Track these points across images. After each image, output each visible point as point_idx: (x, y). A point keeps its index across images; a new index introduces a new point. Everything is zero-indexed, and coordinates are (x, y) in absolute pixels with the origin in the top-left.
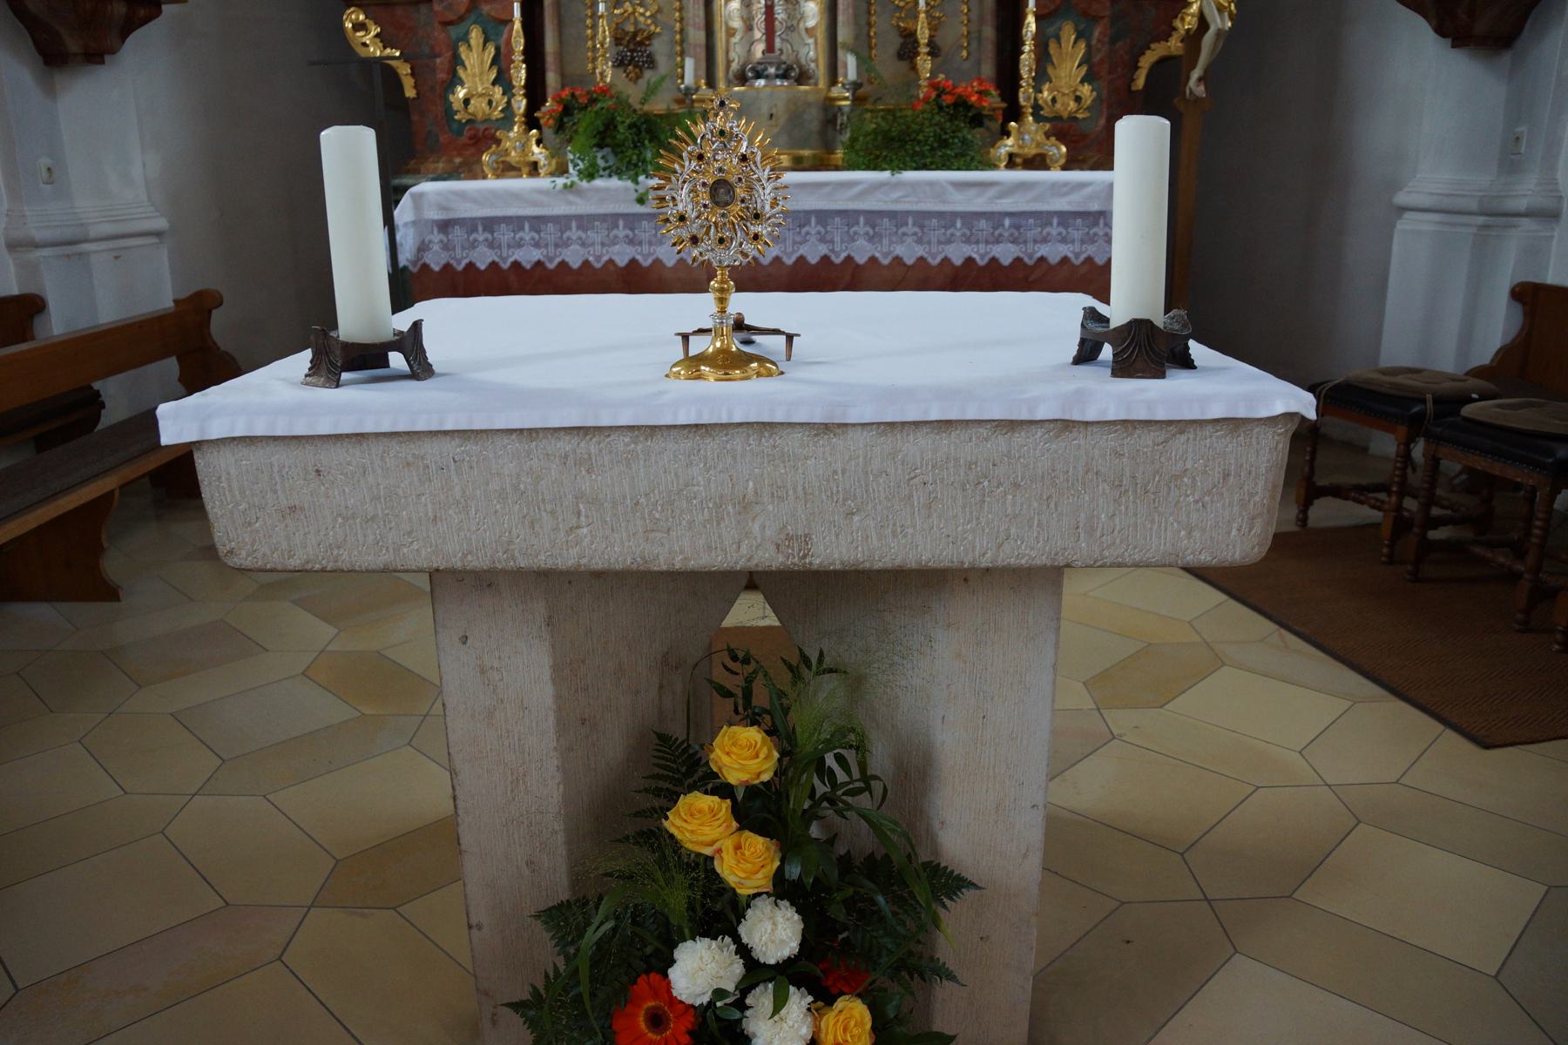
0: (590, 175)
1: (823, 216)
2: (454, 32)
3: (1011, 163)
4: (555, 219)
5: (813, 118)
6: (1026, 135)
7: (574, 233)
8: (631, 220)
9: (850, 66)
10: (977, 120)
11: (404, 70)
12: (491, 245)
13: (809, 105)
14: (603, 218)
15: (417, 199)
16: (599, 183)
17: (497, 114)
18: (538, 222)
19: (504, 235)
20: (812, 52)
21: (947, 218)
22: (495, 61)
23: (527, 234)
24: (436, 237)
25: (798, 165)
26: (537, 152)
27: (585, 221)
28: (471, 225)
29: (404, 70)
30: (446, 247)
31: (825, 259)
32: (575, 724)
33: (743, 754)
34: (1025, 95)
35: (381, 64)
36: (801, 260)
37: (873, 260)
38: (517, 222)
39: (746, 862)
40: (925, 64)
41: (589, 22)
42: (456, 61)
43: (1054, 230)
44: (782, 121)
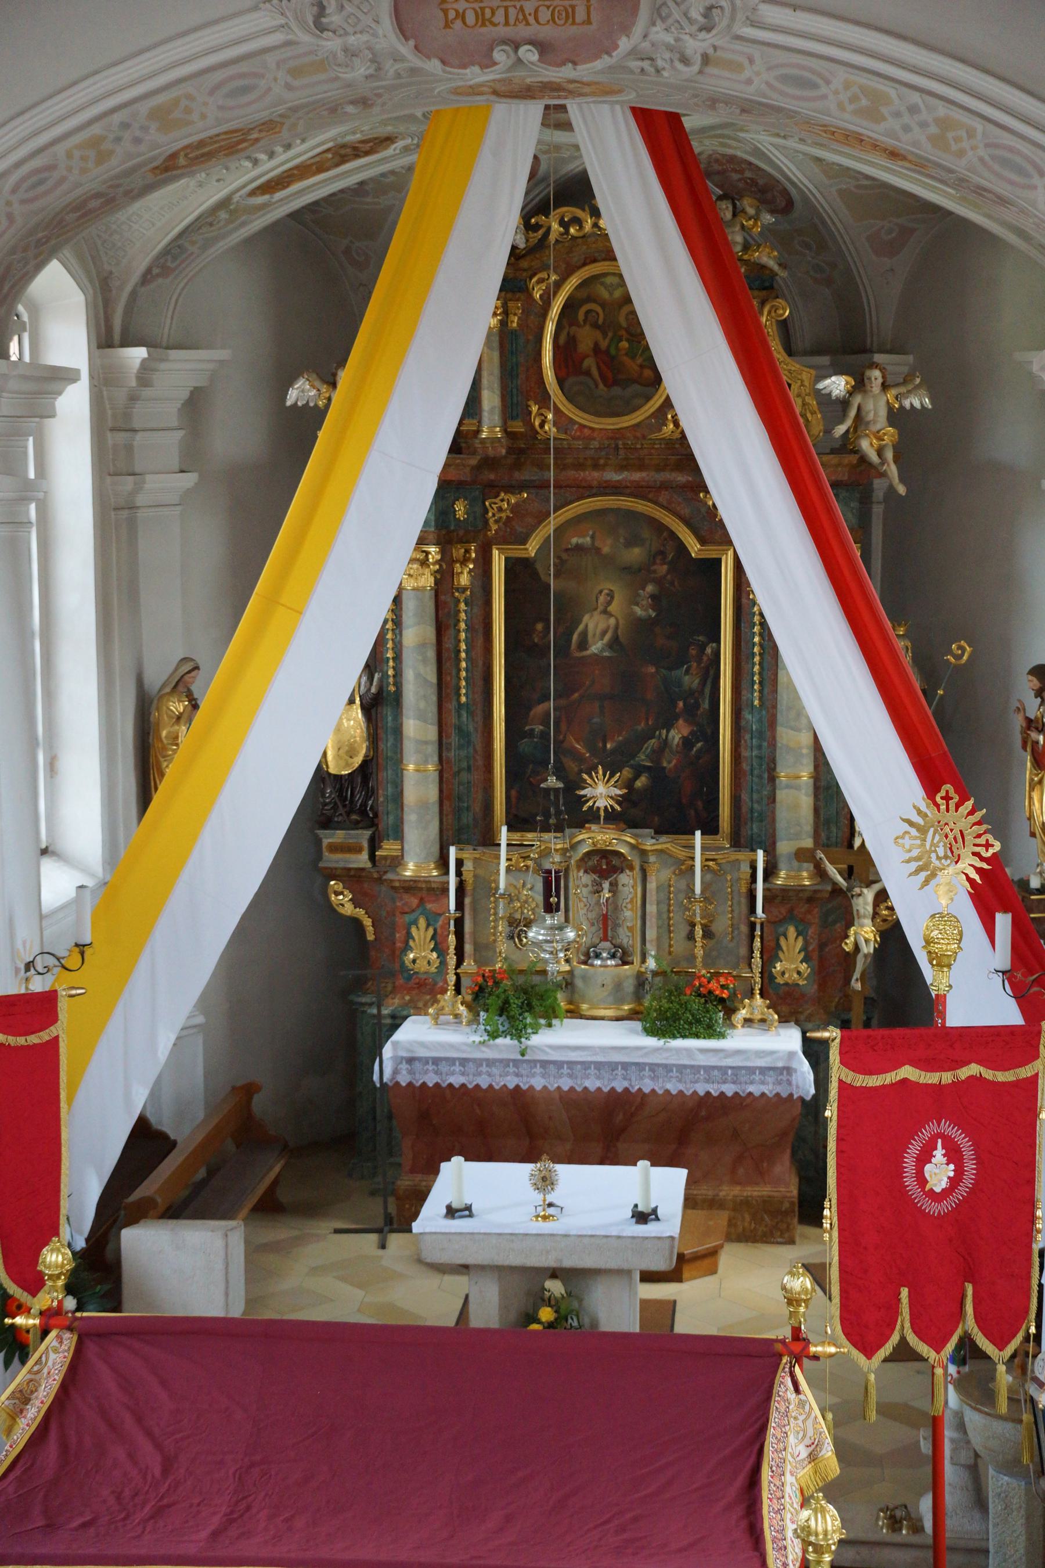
0: (494, 1035)
1: (625, 1066)
2: (407, 918)
4: (474, 1060)
5: (629, 986)
7: (484, 1069)
8: (516, 1063)
11: (367, 922)
12: (436, 1073)
13: (627, 977)
14: (501, 1061)
15: (395, 1044)
16: (500, 1041)
17: (433, 970)
18: (464, 1062)
19: (444, 1067)
21: (696, 1069)
22: (433, 938)
23: (457, 1068)
24: (404, 1066)
27: (490, 1062)
28: (426, 1061)
29: (367, 922)
30: (411, 1072)
31: (626, 1090)
32: (504, 1307)
35: (356, 923)
36: (613, 1089)
37: (653, 1091)
38: (451, 1061)
41: (492, 911)
42: (409, 936)
43: (757, 1077)
44: (610, 988)
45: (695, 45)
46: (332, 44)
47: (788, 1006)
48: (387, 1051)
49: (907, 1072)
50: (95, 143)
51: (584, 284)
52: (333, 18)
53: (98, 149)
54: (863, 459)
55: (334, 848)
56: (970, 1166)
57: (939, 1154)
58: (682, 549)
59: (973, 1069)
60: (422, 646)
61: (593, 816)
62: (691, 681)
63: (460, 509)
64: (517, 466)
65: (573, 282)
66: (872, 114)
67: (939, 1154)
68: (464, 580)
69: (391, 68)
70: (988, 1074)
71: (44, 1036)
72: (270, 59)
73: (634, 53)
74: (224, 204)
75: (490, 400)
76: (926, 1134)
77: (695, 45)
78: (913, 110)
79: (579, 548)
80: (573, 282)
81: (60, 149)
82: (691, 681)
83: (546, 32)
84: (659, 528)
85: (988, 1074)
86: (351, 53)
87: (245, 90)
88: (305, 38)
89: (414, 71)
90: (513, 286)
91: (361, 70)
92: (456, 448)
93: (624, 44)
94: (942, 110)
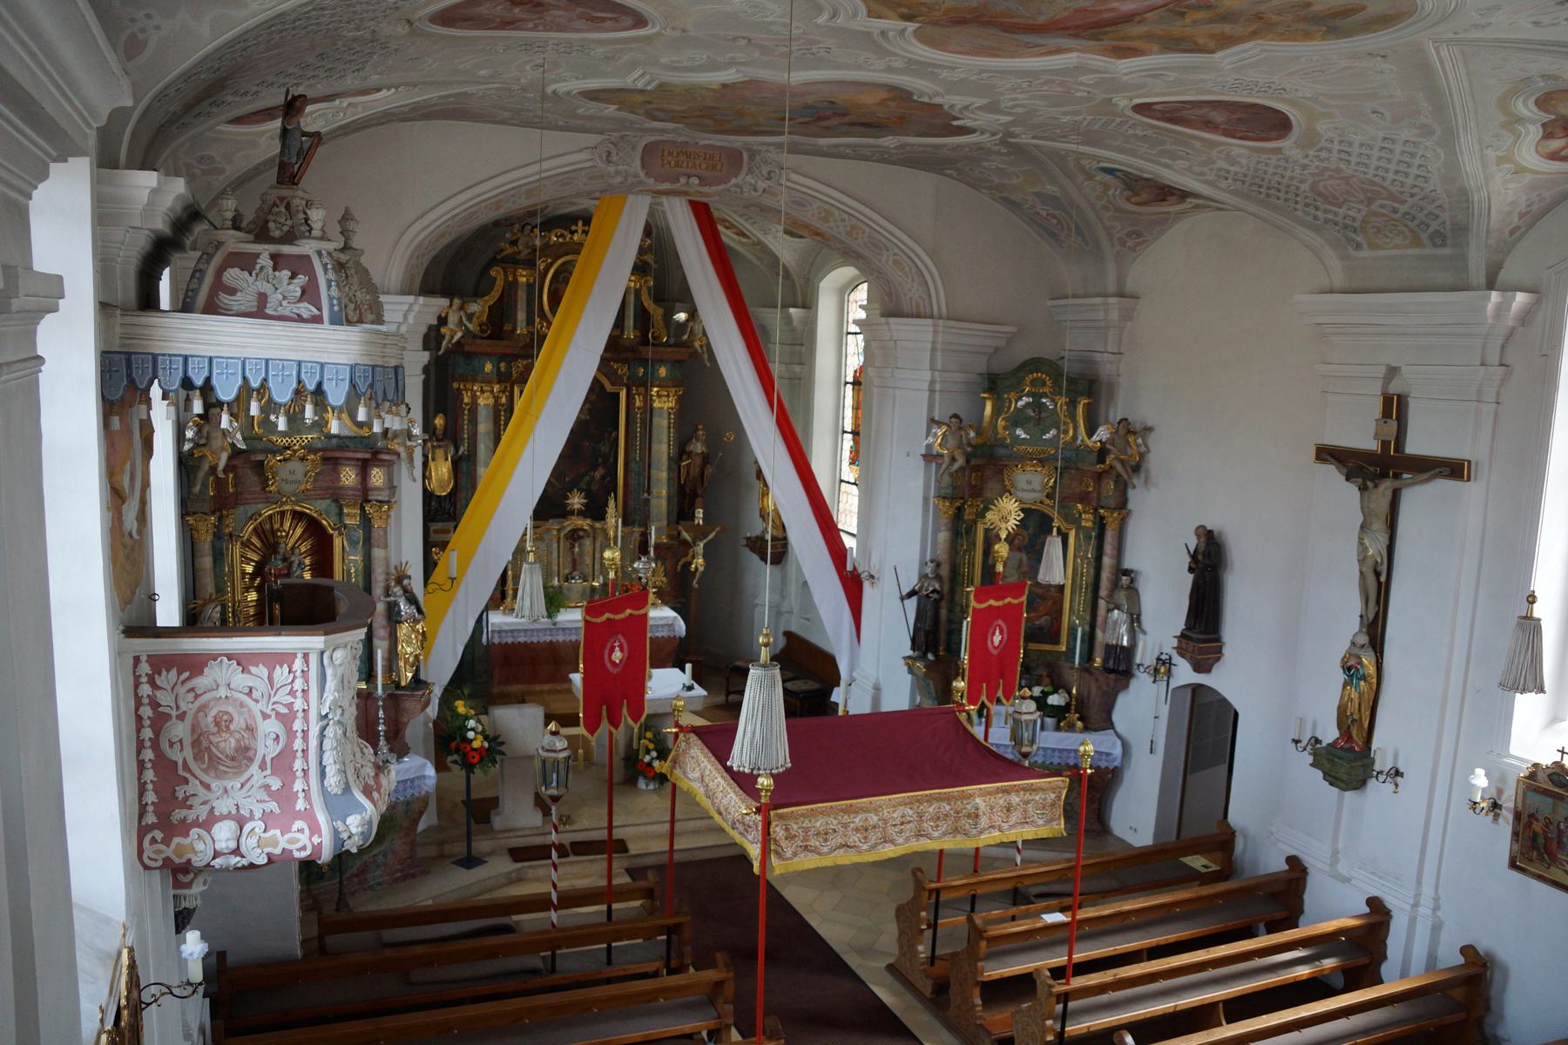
18: (525, 631)
45: (761, 185)
46: (612, 169)
49: (992, 602)
51: (564, 264)
52: (614, 158)
54: (696, 351)
55: (436, 532)
58: (603, 387)
61: (572, 513)
62: (605, 449)
65: (560, 262)
66: (825, 220)
77: (761, 185)
80: (560, 262)
86: (617, 172)
91: (619, 179)
93: (734, 181)
94: (854, 221)
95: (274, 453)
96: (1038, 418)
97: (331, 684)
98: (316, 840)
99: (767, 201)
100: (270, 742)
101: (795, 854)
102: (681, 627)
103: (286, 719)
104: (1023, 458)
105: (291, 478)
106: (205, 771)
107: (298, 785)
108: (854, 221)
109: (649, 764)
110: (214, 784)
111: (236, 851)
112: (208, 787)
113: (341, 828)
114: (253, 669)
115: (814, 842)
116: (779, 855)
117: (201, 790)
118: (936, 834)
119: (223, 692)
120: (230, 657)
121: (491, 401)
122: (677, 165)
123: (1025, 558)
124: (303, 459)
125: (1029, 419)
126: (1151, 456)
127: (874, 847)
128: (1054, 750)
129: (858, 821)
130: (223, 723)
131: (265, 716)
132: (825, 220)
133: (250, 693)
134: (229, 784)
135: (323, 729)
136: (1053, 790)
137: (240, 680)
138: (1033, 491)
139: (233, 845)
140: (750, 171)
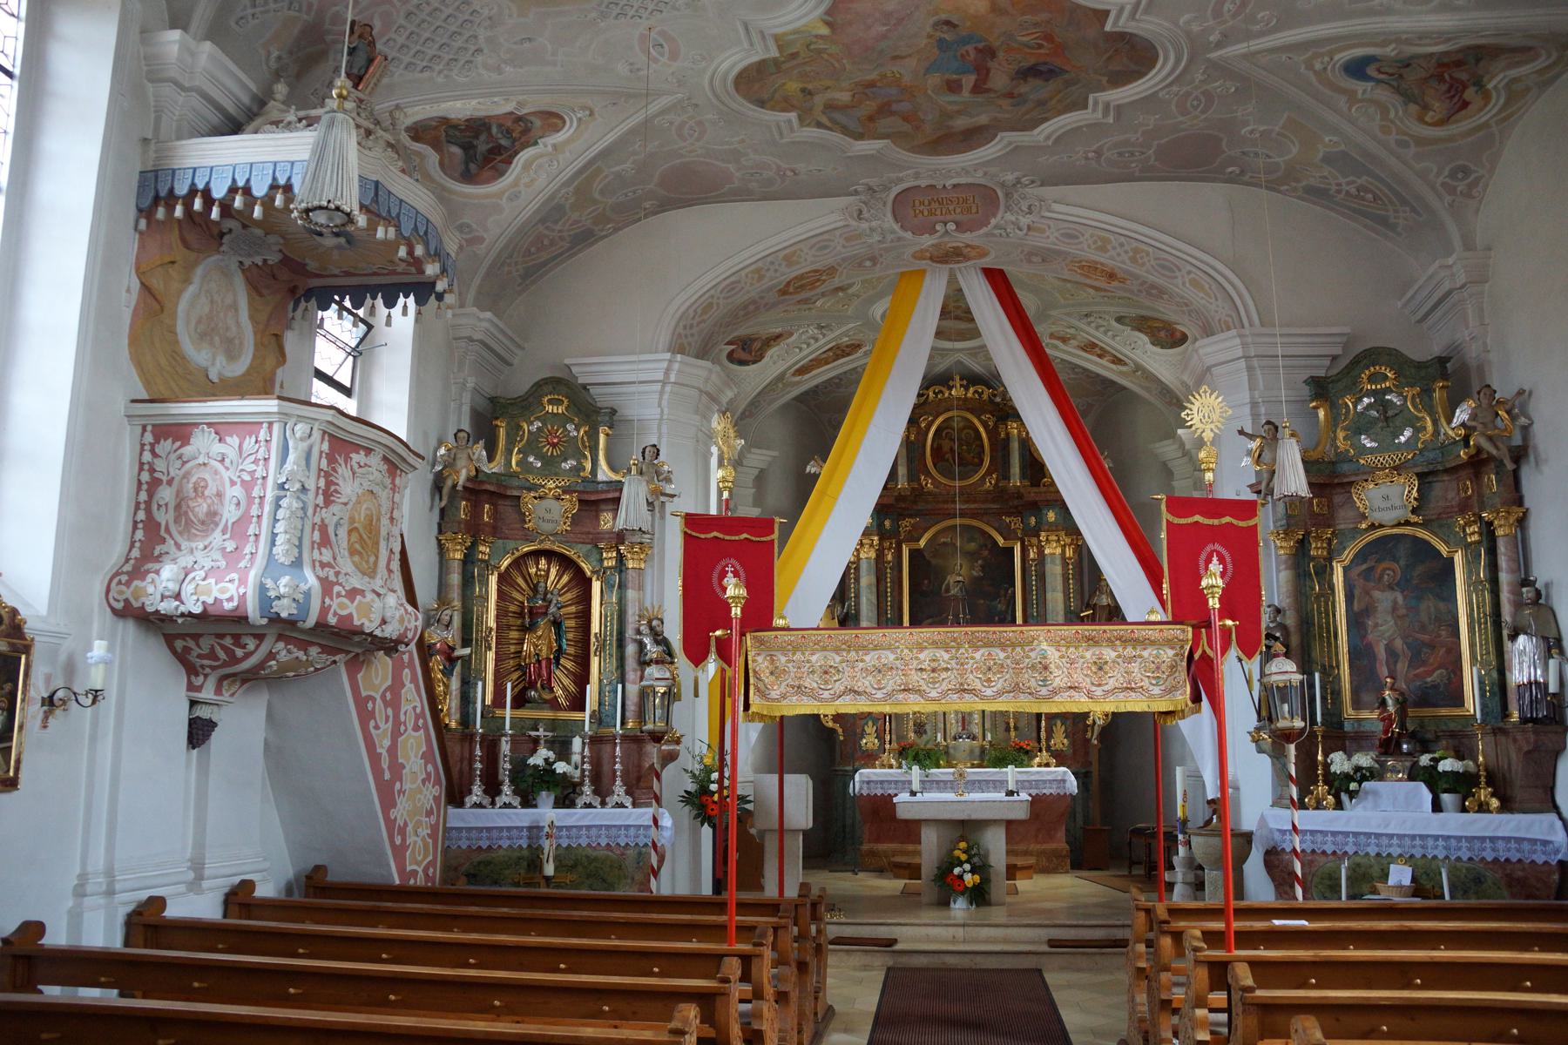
3: (1040, 765)
5: (977, 752)
6: (1044, 756)
9: (989, 737)
10: (1027, 752)
20: (977, 730)
25: (973, 766)
26: (893, 762)
28: (876, 782)
33: (963, 845)
34: (1044, 742)
35: (833, 731)
39: (964, 857)
40: (1013, 734)
45: (1025, 221)
46: (865, 225)
47: (1060, 758)
48: (857, 777)
49: (1197, 518)
50: (758, 270)
52: (866, 215)
53: (759, 274)
56: (1230, 567)
57: (1215, 559)
58: (995, 543)
59: (1227, 519)
60: (869, 586)
63: (887, 523)
64: (915, 502)
65: (940, 419)
67: (1215, 559)
68: (889, 557)
69: (889, 237)
70: (1235, 522)
71: (768, 538)
72: (838, 233)
73: (997, 227)
74: (781, 378)
75: (902, 471)
76: (1209, 548)
77: (1025, 221)
78: (1122, 245)
79: (945, 544)
80: (940, 419)
81: (743, 273)
82: (1001, 607)
83: (959, 217)
84: (984, 533)
85: (1235, 522)
86: (872, 230)
87: (826, 247)
88: (854, 223)
89: (899, 239)
90: (913, 421)
92: (885, 488)
93: (993, 221)
94: (1135, 244)
95: (529, 490)
96: (1388, 419)
97: (291, 457)
98: (242, 591)
99: (1036, 241)
100: (233, 507)
101: (784, 697)
102: (1072, 785)
103: (248, 486)
104: (1370, 473)
105: (548, 516)
106: (180, 533)
107: (248, 549)
108: (1135, 244)
109: (960, 877)
110: (185, 545)
111: (177, 596)
112: (178, 546)
113: (269, 583)
114: (228, 439)
115: (809, 682)
116: (762, 694)
117: (173, 549)
118: (989, 692)
119: (201, 460)
120: (209, 425)
121: (873, 555)
122: (931, 213)
123: (1400, 599)
124: (558, 498)
125: (1374, 421)
126: (1538, 429)
127: (890, 695)
128: (1459, 839)
129: (870, 659)
130: (199, 489)
131: (233, 483)
132: (1103, 249)
133: (222, 461)
134: (194, 545)
135: (279, 499)
136: (1169, 643)
137: (218, 448)
138: (1393, 508)
139: (173, 587)
140: (1008, 208)
